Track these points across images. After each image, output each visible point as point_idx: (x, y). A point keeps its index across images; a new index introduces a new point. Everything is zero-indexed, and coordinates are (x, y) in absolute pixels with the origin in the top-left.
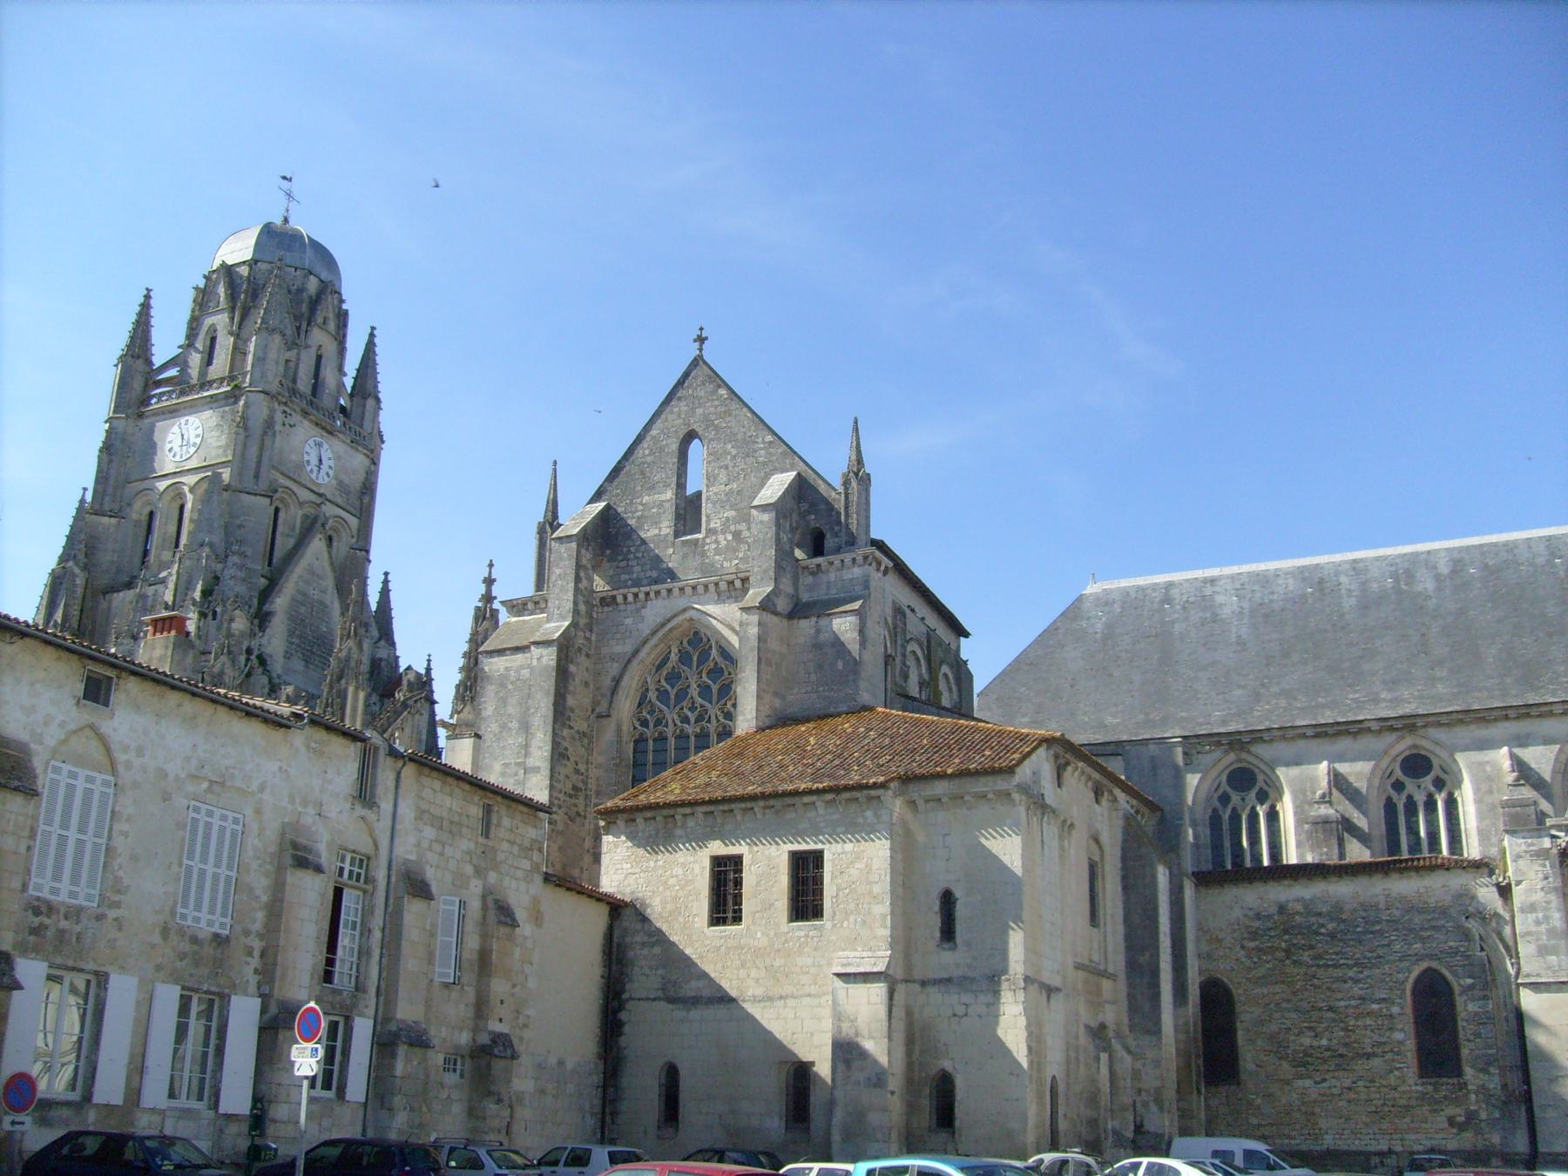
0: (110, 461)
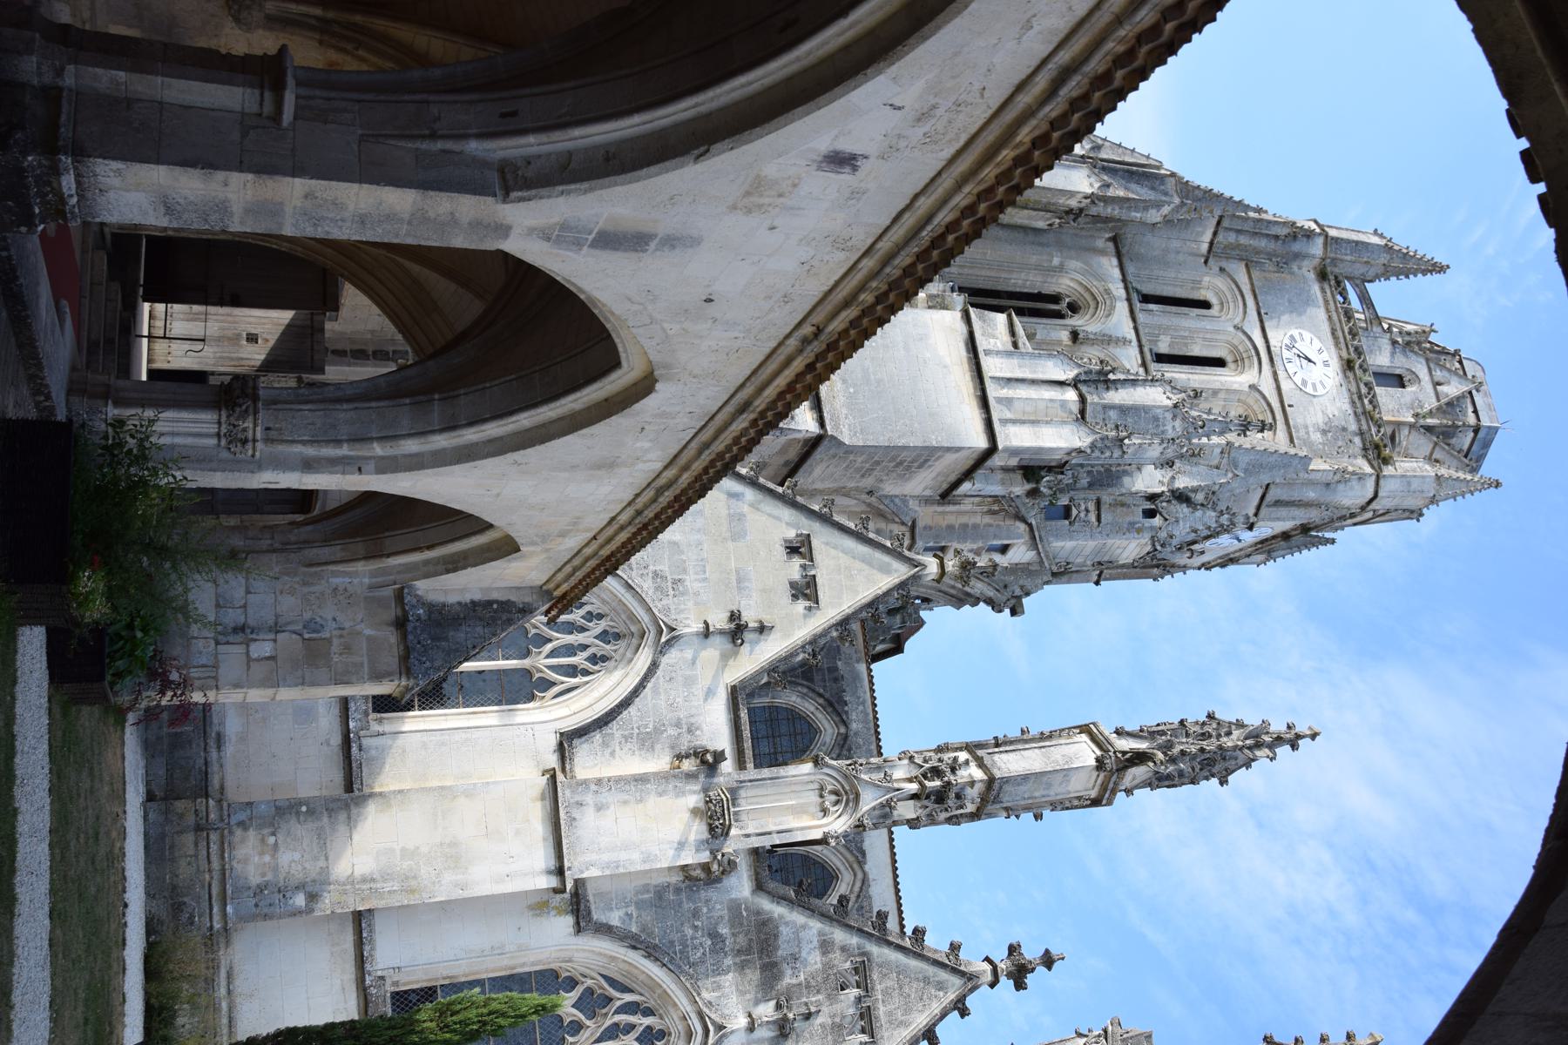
0: (1277, 237)
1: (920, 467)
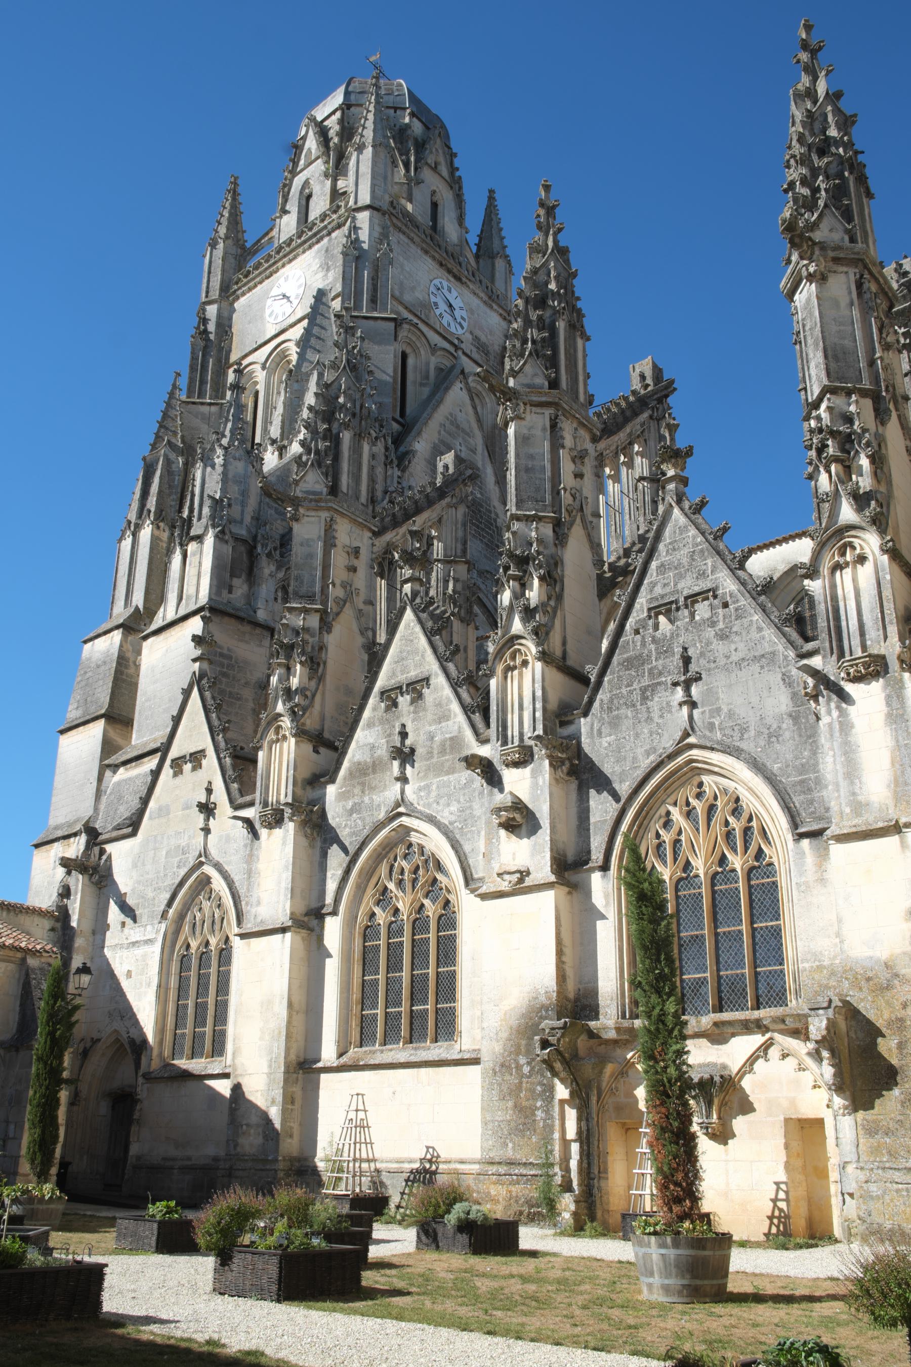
1: (230, 658)
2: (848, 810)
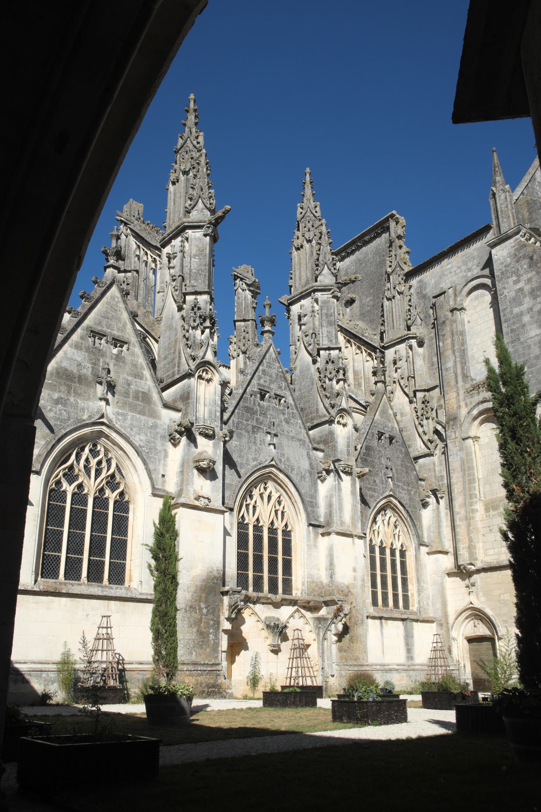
2: (339, 523)
